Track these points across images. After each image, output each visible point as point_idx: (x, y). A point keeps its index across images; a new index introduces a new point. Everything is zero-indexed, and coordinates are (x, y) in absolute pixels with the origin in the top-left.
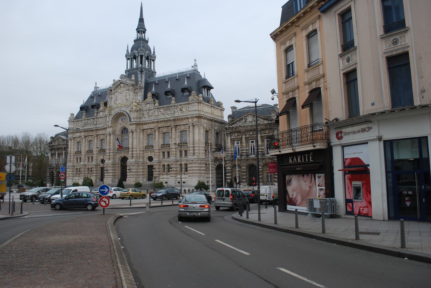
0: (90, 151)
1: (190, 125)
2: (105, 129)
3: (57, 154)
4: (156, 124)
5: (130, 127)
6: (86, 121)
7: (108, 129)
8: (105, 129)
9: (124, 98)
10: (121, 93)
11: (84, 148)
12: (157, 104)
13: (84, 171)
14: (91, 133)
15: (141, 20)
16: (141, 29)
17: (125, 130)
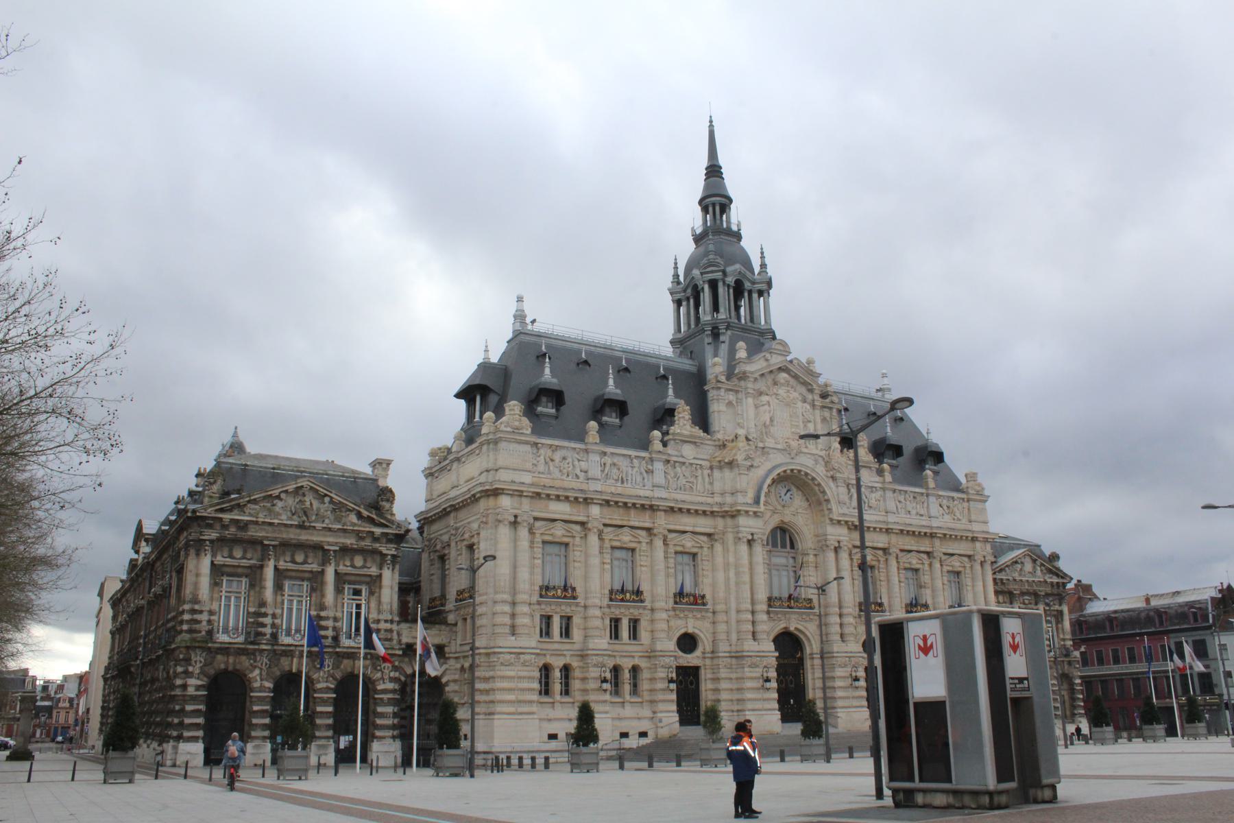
0: (627, 594)
1: (979, 558)
2: (734, 515)
3: (269, 573)
4: (894, 539)
5: (830, 530)
6: (608, 460)
7: (742, 520)
8: (734, 515)
9: (802, 425)
10: (788, 405)
11: (594, 576)
12: (888, 477)
13: (652, 680)
14: (636, 519)
15: (714, 171)
16: (715, 201)
17: (783, 537)
